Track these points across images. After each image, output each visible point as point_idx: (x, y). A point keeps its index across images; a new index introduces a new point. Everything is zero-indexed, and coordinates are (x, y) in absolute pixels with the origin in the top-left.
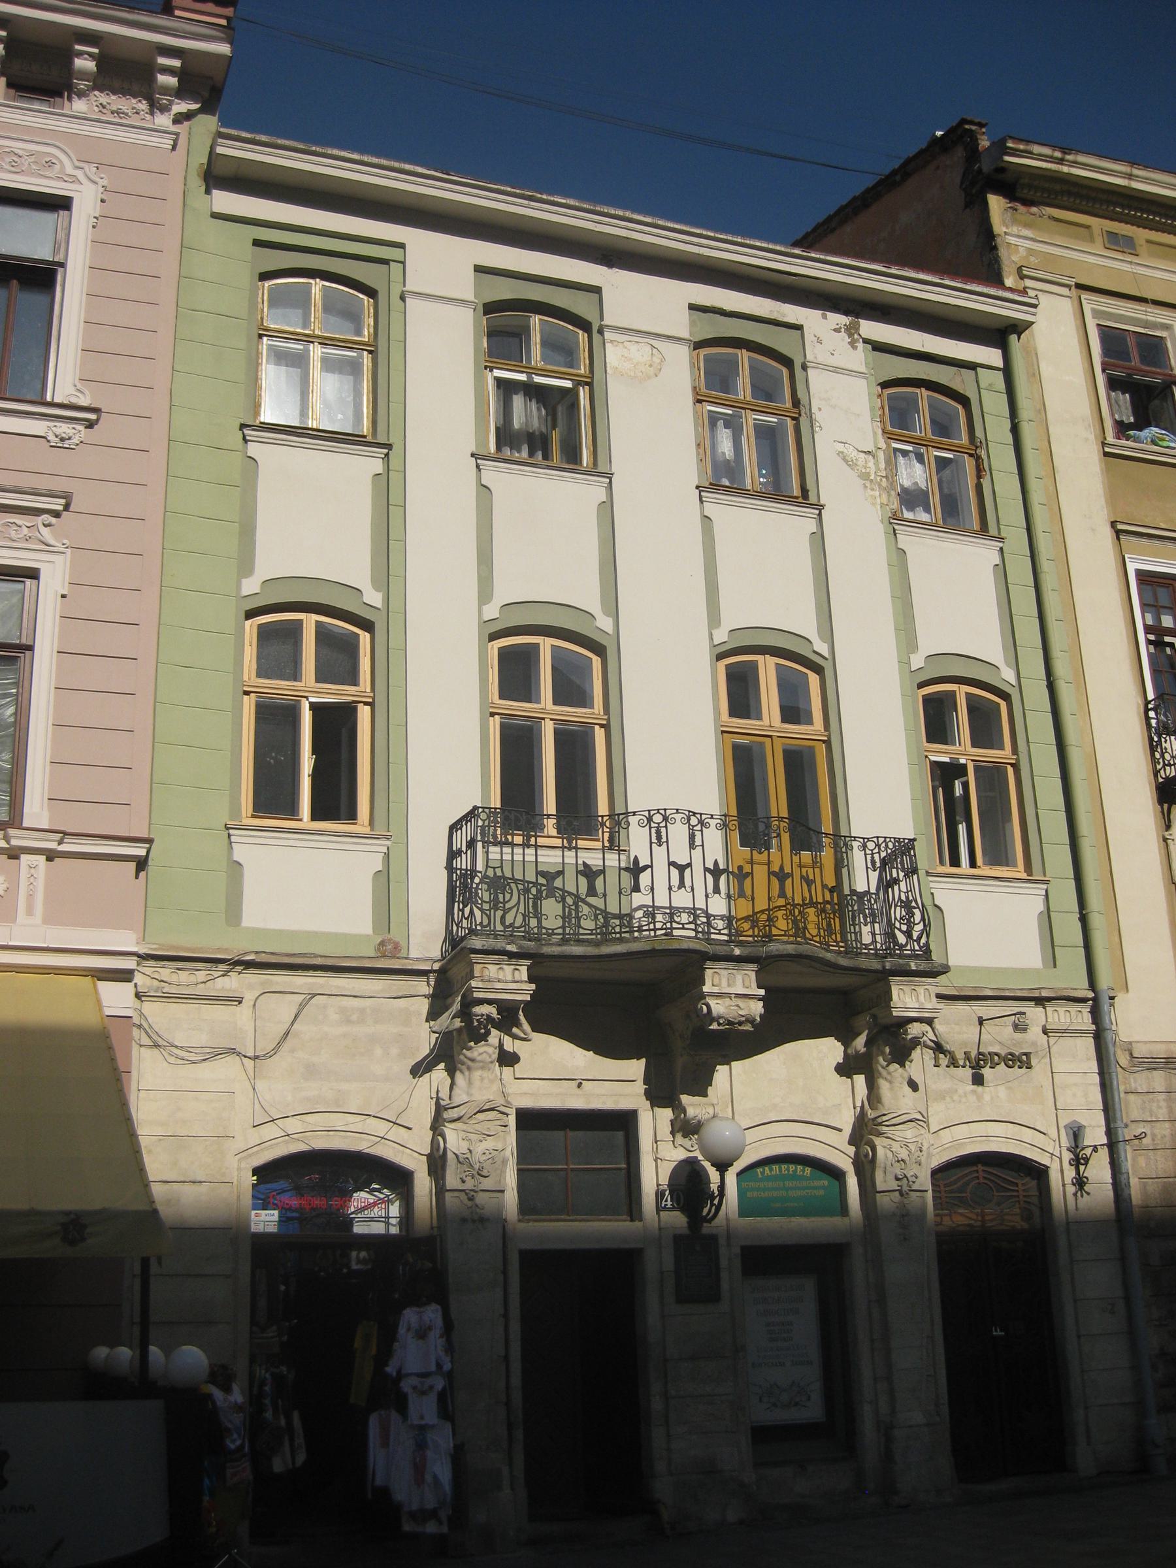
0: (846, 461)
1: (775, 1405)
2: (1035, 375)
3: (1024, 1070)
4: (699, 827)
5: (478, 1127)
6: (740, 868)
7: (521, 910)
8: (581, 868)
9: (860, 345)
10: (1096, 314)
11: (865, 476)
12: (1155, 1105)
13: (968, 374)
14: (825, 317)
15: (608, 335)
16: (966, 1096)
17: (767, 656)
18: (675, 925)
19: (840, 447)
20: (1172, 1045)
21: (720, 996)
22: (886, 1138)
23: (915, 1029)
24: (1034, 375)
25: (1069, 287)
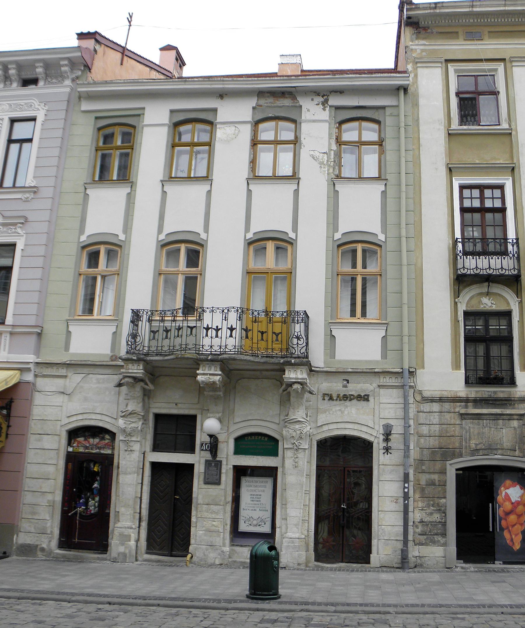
0: (313, 158)
1: (250, 525)
2: (416, 105)
3: (365, 402)
4: (202, 313)
5: (130, 419)
6: (217, 327)
7: (143, 344)
8: (165, 329)
9: (328, 109)
10: (456, 71)
11: (322, 163)
12: (432, 418)
13: (381, 111)
14: (312, 100)
15: (218, 126)
16: (336, 412)
17: (271, 241)
18: (187, 349)
19: (312, 153)
20: (443, 392)
21: (204, 374)
22: (288, 428)
23: (295, 386)
24: (416, 105)
25: (441, 62)
